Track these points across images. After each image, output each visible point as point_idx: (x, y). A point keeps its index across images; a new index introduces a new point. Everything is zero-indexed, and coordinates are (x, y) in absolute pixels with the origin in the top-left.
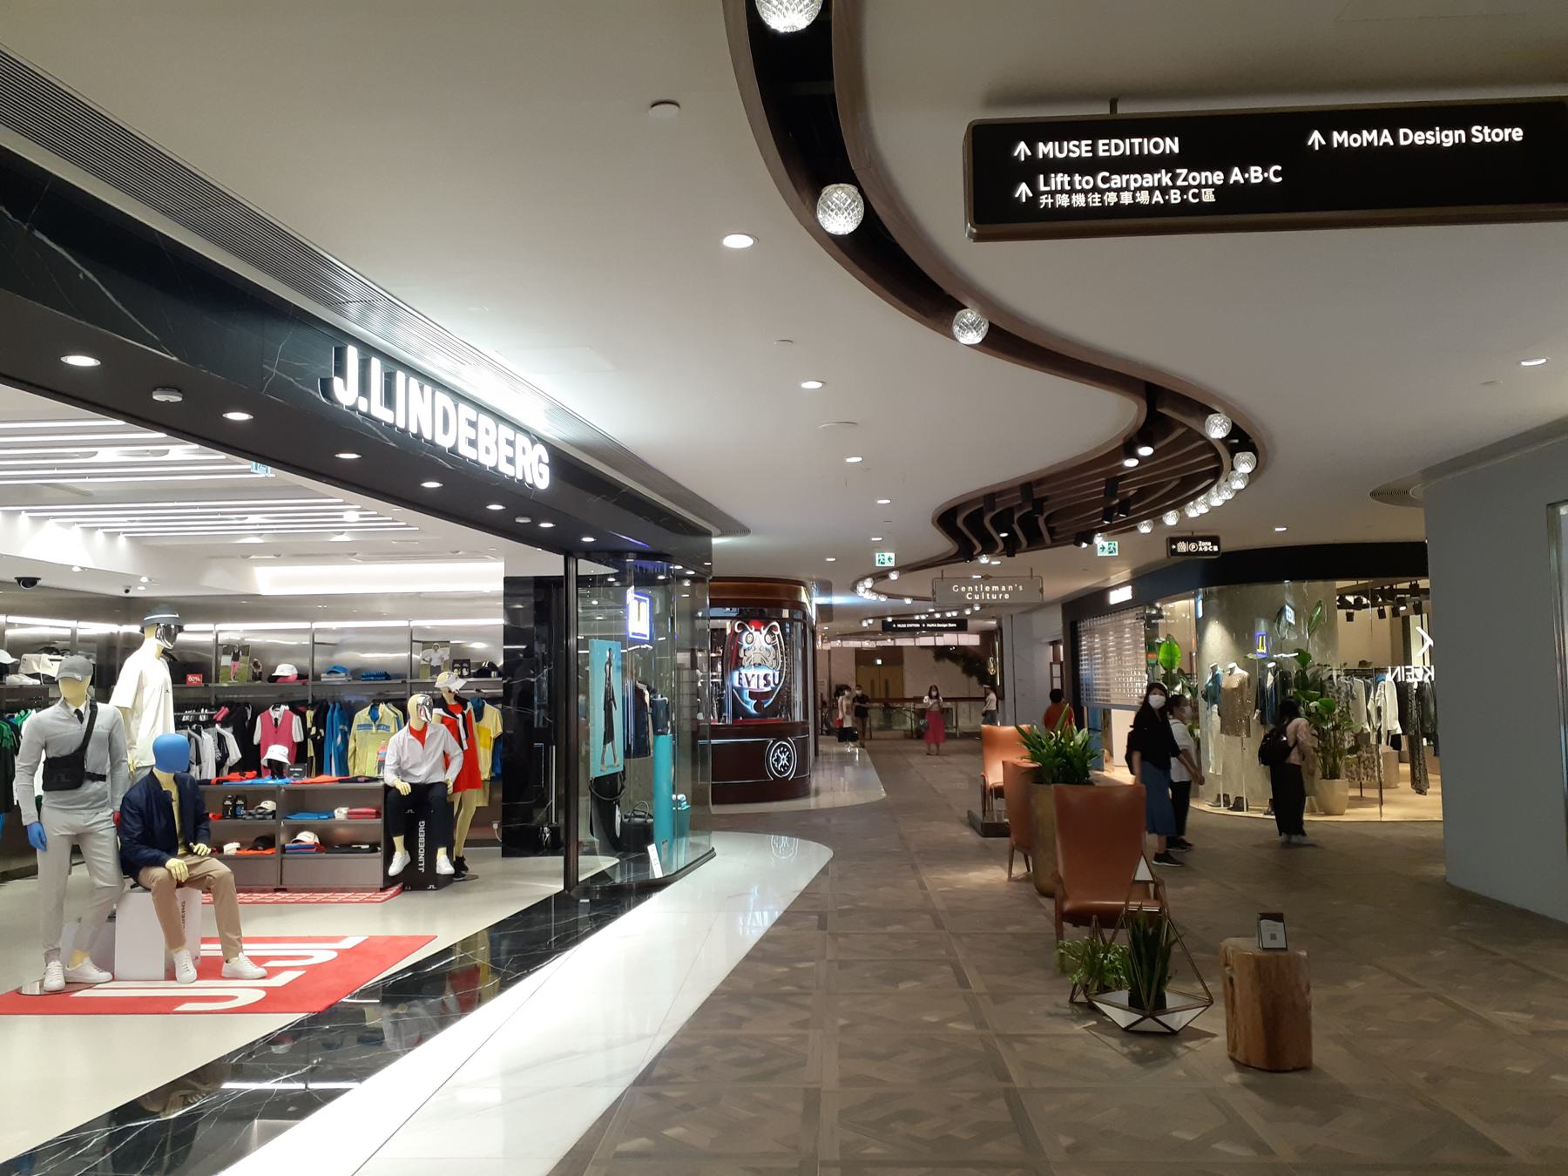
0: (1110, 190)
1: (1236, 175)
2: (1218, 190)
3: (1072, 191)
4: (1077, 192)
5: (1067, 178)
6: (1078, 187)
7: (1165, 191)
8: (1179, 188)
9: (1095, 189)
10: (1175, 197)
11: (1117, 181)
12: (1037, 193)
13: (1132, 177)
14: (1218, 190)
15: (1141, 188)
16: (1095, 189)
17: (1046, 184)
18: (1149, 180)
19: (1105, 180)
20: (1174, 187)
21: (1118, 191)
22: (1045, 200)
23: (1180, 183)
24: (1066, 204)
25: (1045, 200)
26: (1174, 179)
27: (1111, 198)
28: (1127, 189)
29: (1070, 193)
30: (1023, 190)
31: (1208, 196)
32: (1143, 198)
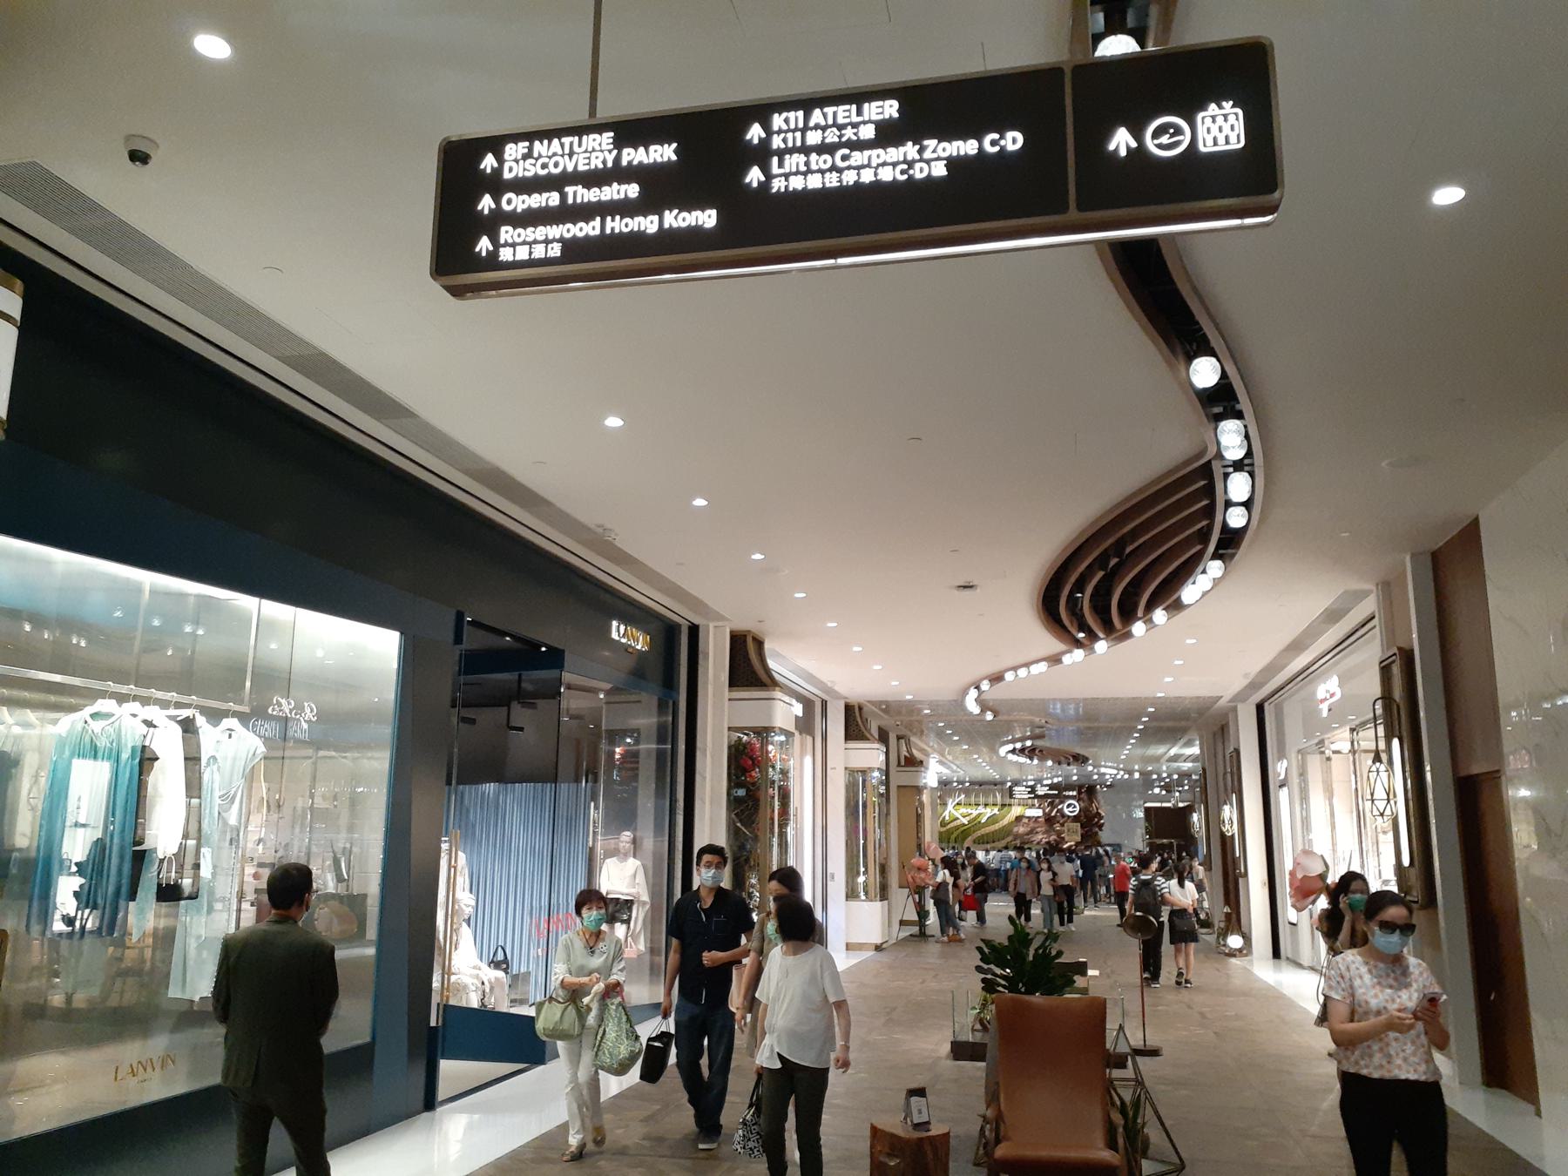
0: (849, 168)
3: (809, 171)
4: (812, 172)
5: (802, 158)
6: (814, 167)
7: (911, 164)
8: (928, 162)
9: (831, 169)
11: (858, 158)
12: (769, 177)
15: (884, 164)
16: (834, 168)
17: (781, 165)
19: (844, 158)
20: (921, 160)
21: (858, 168)
22: (778, 185)
23: (927, 155)
24: (800, 187)
27: (850, 178)
28: (869, 166)
29: (805, 174)
30: (754, 176)
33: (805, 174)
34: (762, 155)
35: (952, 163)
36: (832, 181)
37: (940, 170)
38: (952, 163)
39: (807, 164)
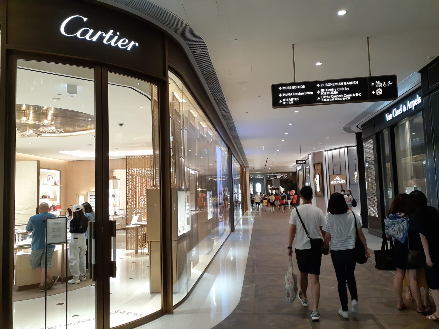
1: (354, 95)
2: (351, 97)
7: (342, 98)
9: (331, 98)
10: (344, 99)
11: (334, 97)
14: (351, 97)
16: (331, 98)
22: (323, 100)
25: (323, 100)
27: (333, 99)
31: (349, 98)
32: (339, 99)
34: (320, 95)
36: (331, 100)
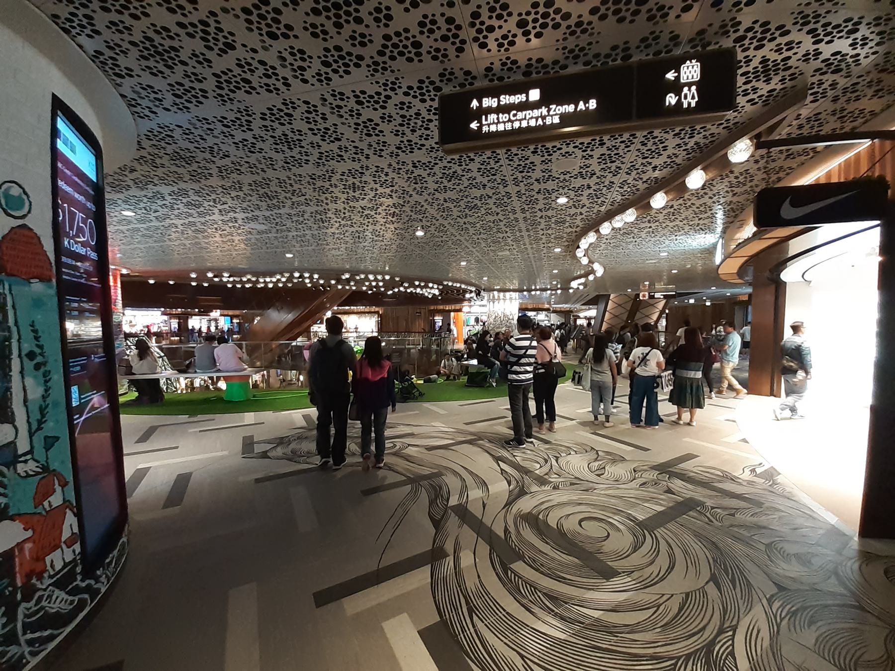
0: (516, 120)
5: (495, 116)
7: (544, 118)
8: (552, 116)
11: (520, 115)
13: (528, 112)
15: (532, 118)
16: (510, 120)
17: (486, 120)
18: (536, 113)
19: (515, 115)
20: (549, 115)
23: (552, 113)
26: (549, 111)
27: (516, 125)
28: (525, 119)
29: (497, 124)
32: (533, 123)
33: (497, 124)
35: (562, 116)
36: (509, 126)
37: (556, 120)
38: (562, 116)
39: (498, 119)
